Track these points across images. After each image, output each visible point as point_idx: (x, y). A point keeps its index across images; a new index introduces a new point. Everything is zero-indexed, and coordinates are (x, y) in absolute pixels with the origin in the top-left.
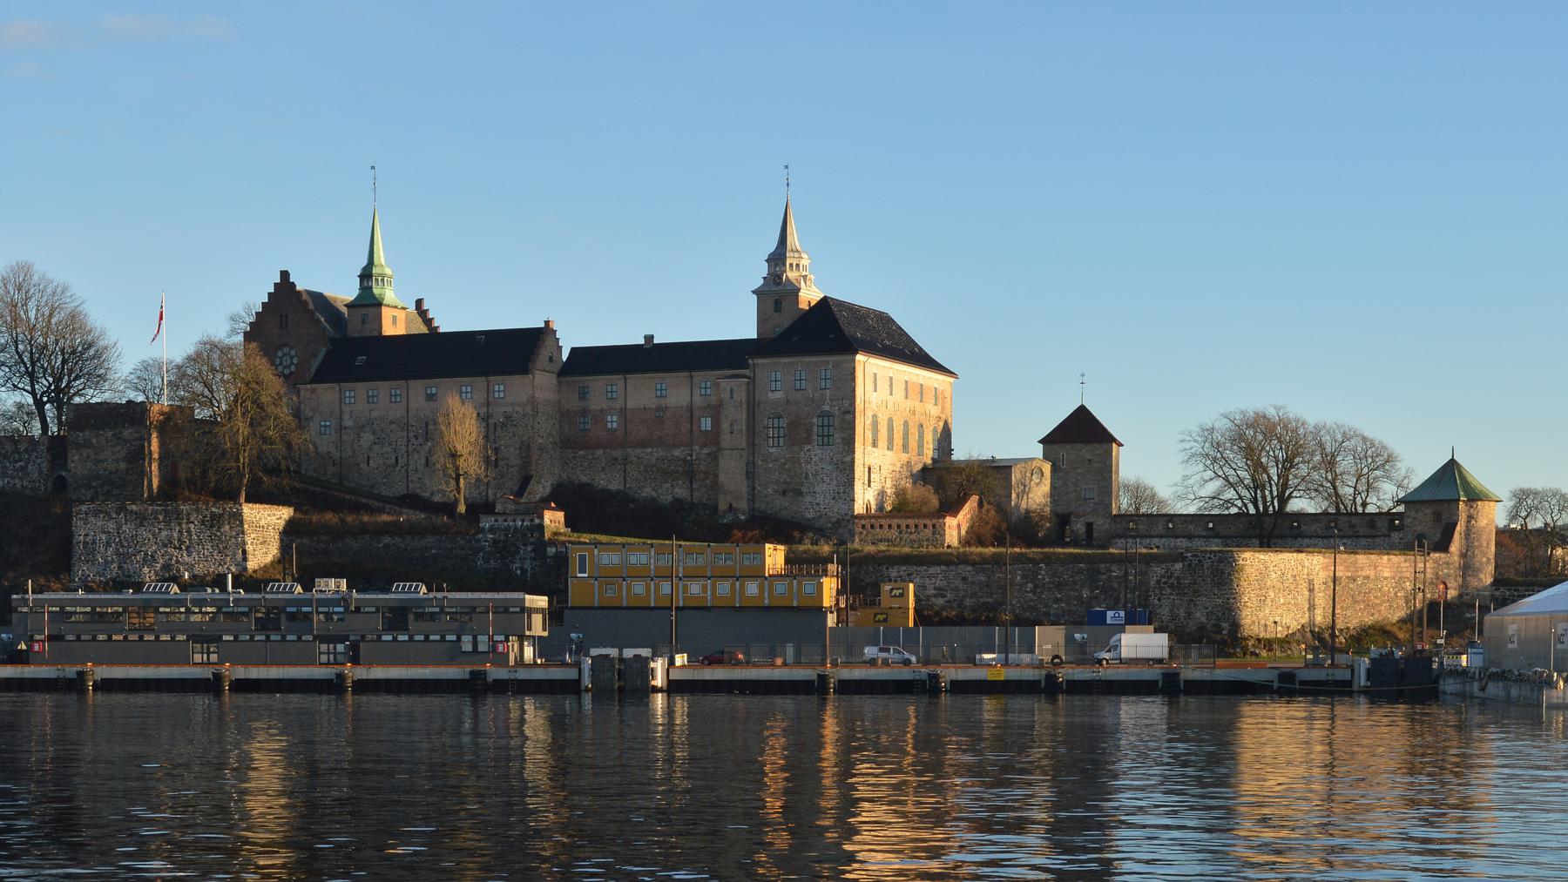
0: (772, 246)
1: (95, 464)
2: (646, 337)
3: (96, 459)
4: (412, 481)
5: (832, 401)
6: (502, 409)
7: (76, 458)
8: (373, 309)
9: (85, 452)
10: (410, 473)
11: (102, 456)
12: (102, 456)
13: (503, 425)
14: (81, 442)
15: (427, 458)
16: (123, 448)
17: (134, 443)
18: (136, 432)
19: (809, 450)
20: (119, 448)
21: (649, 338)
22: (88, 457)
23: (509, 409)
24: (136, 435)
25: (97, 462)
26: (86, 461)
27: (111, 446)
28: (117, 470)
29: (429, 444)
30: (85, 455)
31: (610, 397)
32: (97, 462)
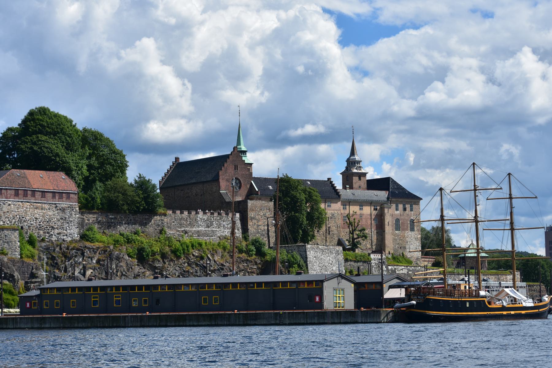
5: (414, 215)
6: (331, 212)
7: (251, 223)
9: (254, 221)
11: (260, 223)
12: (260, 223)
13: (331, 218)
19: (407, 233)
20: (265, 220)
22: (255, 224)
23: (333, 212)
25: (258, 226)
28: (264, 230)
32: (258, 226)
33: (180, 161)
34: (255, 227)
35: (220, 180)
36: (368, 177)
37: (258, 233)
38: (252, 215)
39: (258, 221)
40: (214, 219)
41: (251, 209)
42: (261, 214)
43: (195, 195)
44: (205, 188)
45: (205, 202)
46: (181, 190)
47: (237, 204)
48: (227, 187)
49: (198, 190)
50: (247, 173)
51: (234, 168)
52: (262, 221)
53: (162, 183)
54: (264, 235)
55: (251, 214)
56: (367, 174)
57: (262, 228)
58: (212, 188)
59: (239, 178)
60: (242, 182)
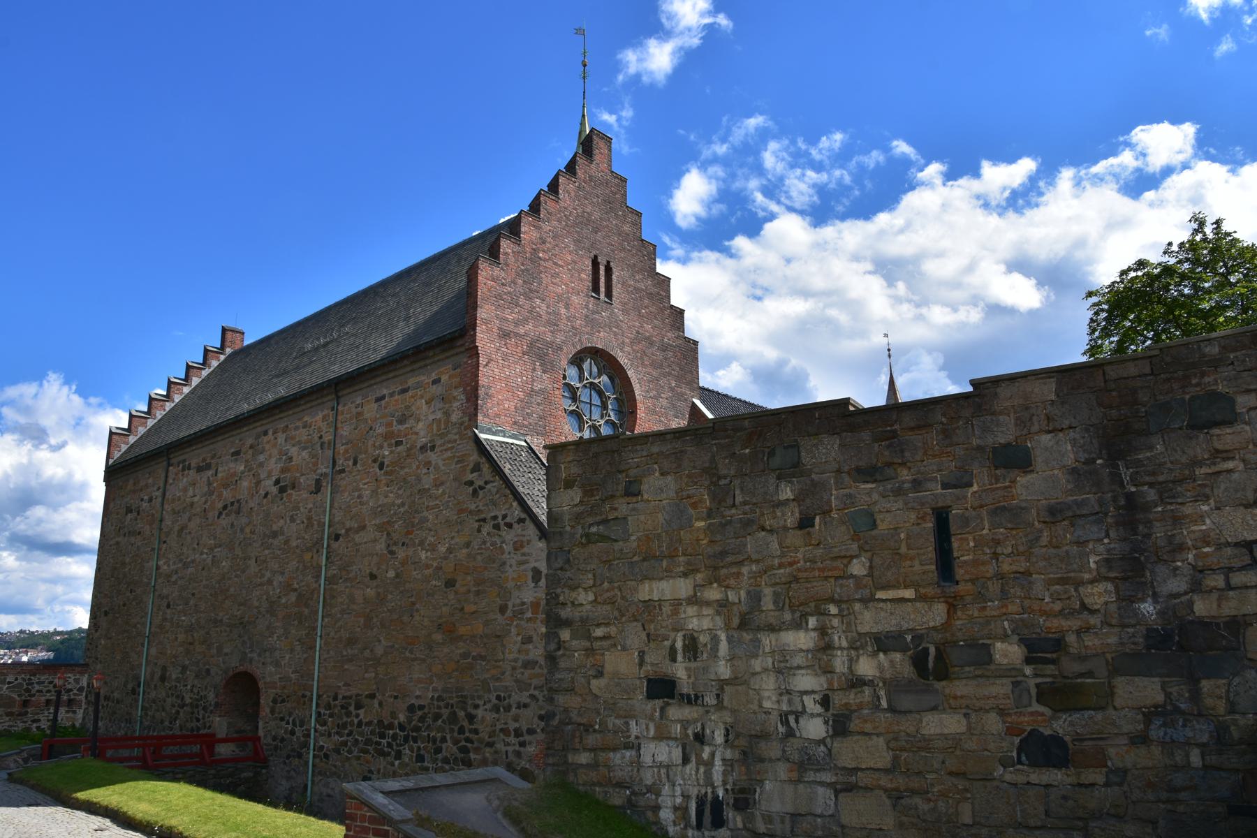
35: (484, 339)
43: (274, 490)
44: (345, 431)
45: (337, 537)
46: (200, 469)
48: (536, 410)
49: (294, 451)
51: (586, 276)
53: (124, 448)
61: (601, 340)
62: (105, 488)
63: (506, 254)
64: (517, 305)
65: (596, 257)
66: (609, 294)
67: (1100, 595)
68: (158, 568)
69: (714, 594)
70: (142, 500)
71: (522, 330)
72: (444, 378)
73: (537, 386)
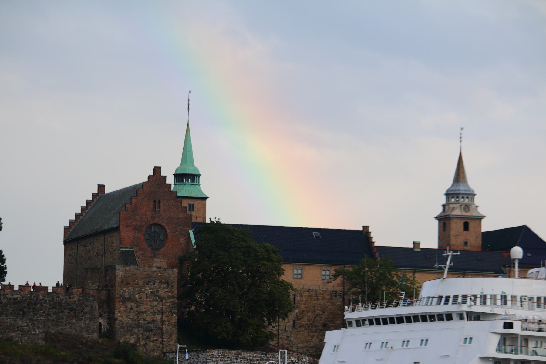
0: (448, 183)
1: (136, 315)
2: (414, 243)
3: (137, 311)
4: (281, 338)
7: (122, 309)
8: (199, 201)
9: (129, 304)
10: (280, 332)
11: (143, 309)
12: (143, 309)
14: (127, 296)
15: (294, 322)
16: (158, 304)
17: (169, 301)
18: (169, 292)
20: (155, 303)
21: (416, 244)
22: (132, 309)
24: (170, 294)
25: (139, 313)
26: (130, 312)
27: (150, 301)
28: (154, 321)
29: (297, 311)
30: (129, 307)
31: (300, 276)
33: (107, 191)
34: (132, 315)
36: (487, 226)
37: (138, 326)
38: (127, 293)
39: (139, 303)
40: (37, 300)
41: (122, 282)
42: (146, 292)
43: (96, 255)
47: (104, 272)
50: (181, 215)
51: (152, 207)
52: (150, 303)
53: (69, 233)
54: (151, 331)
55: (124, 291)
56: (483, 221)
57: (149, 318)
58: (113, 243)
59: (163, 224)
60: (168, 231)
61: (156, 221)
62: (64, 247)
63: (128, 208)
64: (131, 218)
65: (155, 201)
66: (159, 207)
67: (104, 282)
68: (77, 273)
69: (91, 282)
70: (73, 253)
71: (132, 224)
72: (117, 235)
73: (136, 236)
